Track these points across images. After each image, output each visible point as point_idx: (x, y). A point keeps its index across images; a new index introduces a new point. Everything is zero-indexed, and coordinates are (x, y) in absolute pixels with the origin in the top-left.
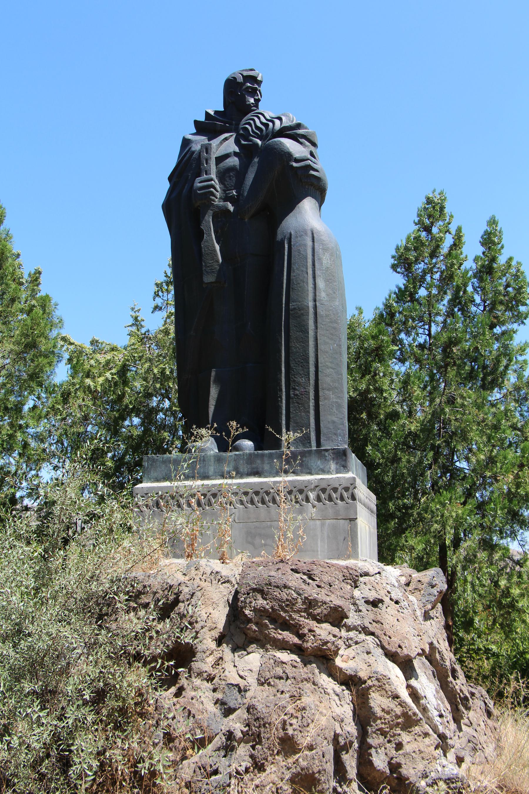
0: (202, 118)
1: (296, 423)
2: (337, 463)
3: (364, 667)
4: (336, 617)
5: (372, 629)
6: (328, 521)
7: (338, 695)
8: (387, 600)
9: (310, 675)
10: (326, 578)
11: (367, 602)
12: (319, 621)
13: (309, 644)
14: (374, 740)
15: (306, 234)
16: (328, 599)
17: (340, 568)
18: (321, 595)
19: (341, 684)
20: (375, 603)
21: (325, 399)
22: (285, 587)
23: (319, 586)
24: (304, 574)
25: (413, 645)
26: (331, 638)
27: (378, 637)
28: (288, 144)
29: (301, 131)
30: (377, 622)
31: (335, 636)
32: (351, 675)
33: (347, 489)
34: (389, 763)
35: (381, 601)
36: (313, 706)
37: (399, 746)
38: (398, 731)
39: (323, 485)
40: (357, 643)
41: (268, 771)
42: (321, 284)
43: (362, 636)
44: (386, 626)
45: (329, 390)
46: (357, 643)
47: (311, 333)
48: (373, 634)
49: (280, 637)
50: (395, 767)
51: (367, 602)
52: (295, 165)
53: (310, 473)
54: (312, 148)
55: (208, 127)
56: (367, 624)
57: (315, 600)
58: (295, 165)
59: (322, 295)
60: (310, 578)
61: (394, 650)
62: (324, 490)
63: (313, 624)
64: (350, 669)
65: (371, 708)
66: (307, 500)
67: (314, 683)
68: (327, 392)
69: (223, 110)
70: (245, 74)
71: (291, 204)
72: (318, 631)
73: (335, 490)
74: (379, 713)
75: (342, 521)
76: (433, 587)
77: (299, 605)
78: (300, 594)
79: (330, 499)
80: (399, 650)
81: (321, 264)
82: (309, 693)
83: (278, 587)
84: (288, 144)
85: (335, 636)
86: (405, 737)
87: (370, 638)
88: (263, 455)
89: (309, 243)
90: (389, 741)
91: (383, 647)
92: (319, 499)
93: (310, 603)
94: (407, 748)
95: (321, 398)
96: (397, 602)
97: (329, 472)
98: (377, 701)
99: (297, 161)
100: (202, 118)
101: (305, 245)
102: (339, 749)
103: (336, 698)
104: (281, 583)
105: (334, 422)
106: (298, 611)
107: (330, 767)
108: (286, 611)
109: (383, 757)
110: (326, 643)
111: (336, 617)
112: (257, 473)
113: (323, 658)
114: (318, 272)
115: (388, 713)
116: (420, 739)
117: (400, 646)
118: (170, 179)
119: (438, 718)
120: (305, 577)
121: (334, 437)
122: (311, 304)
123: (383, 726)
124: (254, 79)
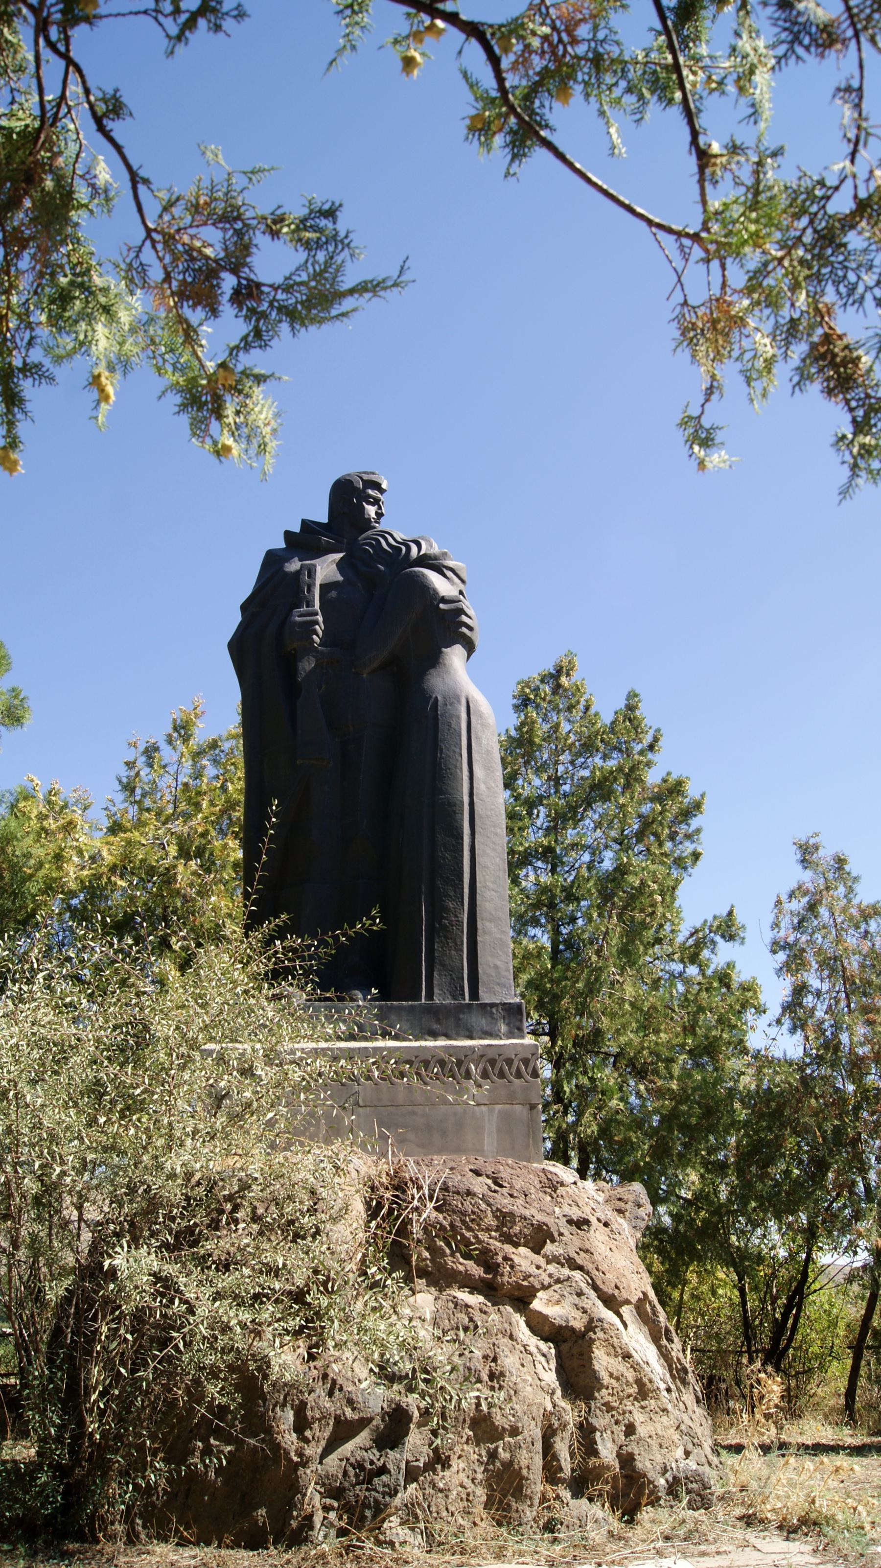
0: (296, 528)
1: (443, 965)
2: (508, 1024)
3: (578, 1314)
4: (538, 1238)
5: (579, 1261)
6: (498, 1107)
7: (544, 1355)
8: (593, 1220)
10: (518, 1184)
11: (570, 1222)
12: (516, 1245)
13: (506, 1279)
15: (459, 701)
16: (527, 1213)
17: (535, 1172)
18: (518, 1207)
19: (546, 1340)
21: (485, 933)
22: (469, 1193)
23: (511, 1196)
24: (488, 1177)
25: (633, 1286)
26: (533, 1270)
27: (588, 1273)
28: (434, 578)
29: (450, 563)
30: (587, 1251)
31: (538, 1267)
32: (560, 1326)
33: (526, 1062)
34: (619, 1455)
35: (587, 1222)
37: (630, 1430)
38: (628, 1405)
39: (491, 1054)
40: (558, 1281)
41: (454, 1468)
43: (566, 1271)
44: (596, 1257)
45: (490, 921)
46: (558, 1281)
48: (581, 1268)
49: (461, 1268)
50: (627, 1460)
51: (570, 1222)
52: (442, 606)
53: (471, 1037)
54: (462, 586)
55: (306, 541)
56: (573, 1255)
57: (512, 1214)
58: (442, 606)
60: (496, 1183)
61: (610, 1292)
62: (493, 1062)
63: (508, 1249)
64: (561, 1317)
65: (594, 1371)
66: (468, 1075)
67: (511, 1337)
68: (488, 924)
69: (324, 519)
70: (365, 477)
71: (433, 659)
72: (517, 1260)
73: (509, 1062)
74: (606, 1380)
75: (519, 1108)
77: (490, 1220)
78: (489, 1205)
79: (502, 1075)
80: (616, 1292)
81: (480, 744)
82: (507, 1352)
83: (458, 1193)
84: (434, 578)
85: (538, 1267)
86: (638, 1417)
87: (577, 1275)
88: (401, 1008)
89: (464, 716)
90: (617, 1422)
91: (595, 1287)
92: (485, 1075)
93: (505, 1218)
95: (480, 932)
96: (606, 1225)
97: (498, 1037)
98: (603, 1361)
99: (444, 600)
100: (296, 528)
102: (548, 1435)
103: (543, 1359)
104: (462, 1188)
105: (496, 967)
106: (488, 1230)
107: (538, 1461)
108: (469, 1229)
109: (610, 1444)
110: (526, 1277)
111: (538, 1238)
113: (521, 1299)
115: (617, 1379)
117: (617, 1287)
118: (244, 607)
119: (665, 1393)
120: (489, 1182)
121: (497, 988)
122: (466, 799)
123: (610, 1399)
124: (377, 486)
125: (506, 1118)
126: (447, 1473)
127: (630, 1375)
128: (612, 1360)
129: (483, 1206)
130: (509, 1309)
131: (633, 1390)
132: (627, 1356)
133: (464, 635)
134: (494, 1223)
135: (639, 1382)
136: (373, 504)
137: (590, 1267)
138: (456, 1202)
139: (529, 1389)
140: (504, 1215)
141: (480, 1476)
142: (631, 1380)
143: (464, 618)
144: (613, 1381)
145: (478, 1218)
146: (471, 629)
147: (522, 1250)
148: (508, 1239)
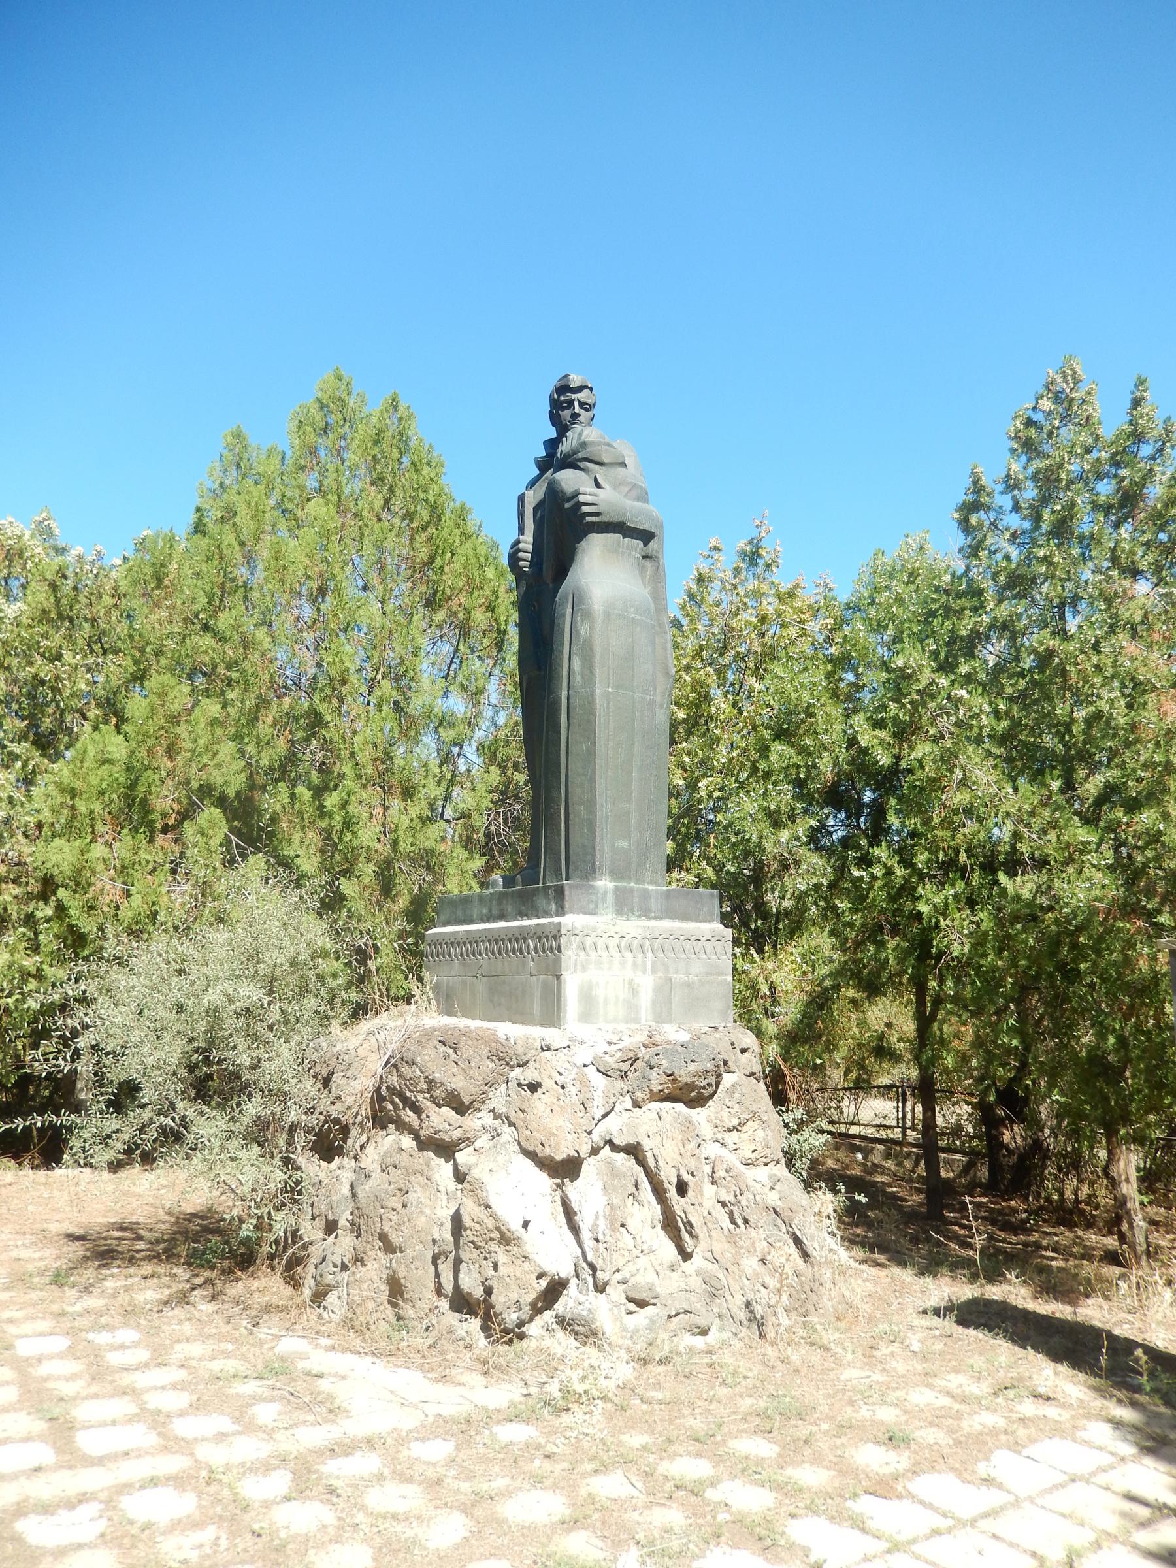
8: (547, 1083)
9: (424, 1167)
14: (467, 1254)
20: (534, 1087)
29: (580, 455)
36: (414, 1204)
37: (496, 1267)
38: (494, 1247)
41: (369, 1266)
42: (577, 664)
44: (530, 1117)
47: (563, 731)
49: (407, 1119)
56: (512, 1115)
58: (567, 505)
59: (577, 679)
61: (531, 1148)
76: (652, 1067)
86: (502, 1258)
90: (486, 1259)
93: (431, 1083)
94: (502, 1270)
96: (563, 1087)
101: (564, 615)
103: (444, 1197)
105: (584, 846)
106: (422, 1092)
108: (411, 1091)
109: (475, 1275)
112: (502, 917)
114: (574, 649)
116: (519, 1262)
123: (475, 1239)
125: (545, 985)
126: (364, 1269)
127: (490, 1223)
128: (476, 1208)
129: (418, 1073)
130: (431, 1154)
131: (496, 1235)
132: (488, 1207)
133: (593, 523)
134: (425, 1087)
135: (498, 1229)
136: (568, 408)
137: (520, 1124)
138: (406, 1070)
139: (423, 1219)
140: (431, 1081)
141: (385, 1277)
142: (491, 1227)
143: (585, 509)
144: (477, 1227)
145: (415, 1084)
146: (598, 514)
147: (445, 1109)
148: (433, 1100)
